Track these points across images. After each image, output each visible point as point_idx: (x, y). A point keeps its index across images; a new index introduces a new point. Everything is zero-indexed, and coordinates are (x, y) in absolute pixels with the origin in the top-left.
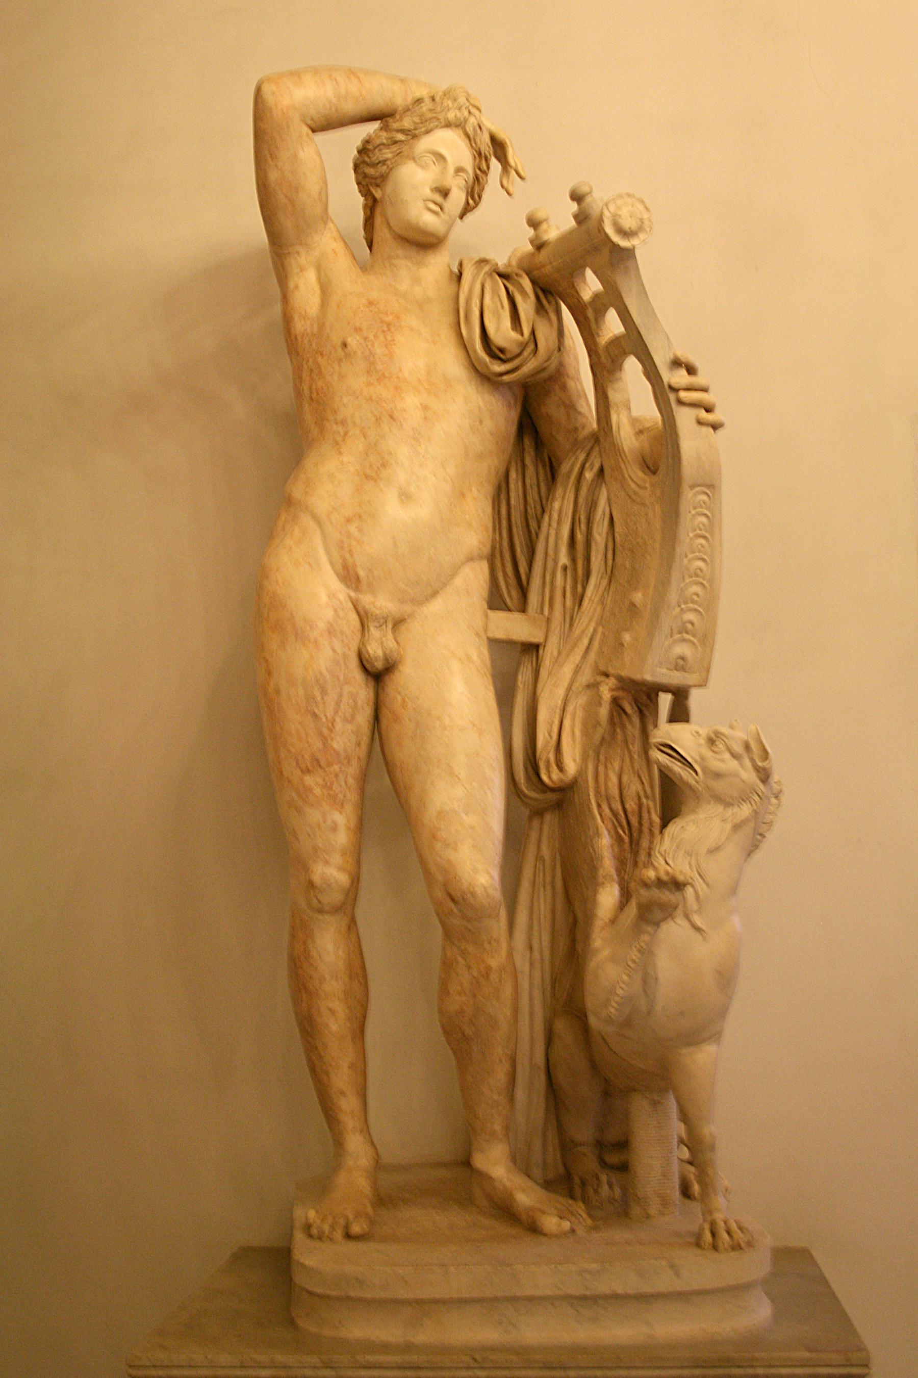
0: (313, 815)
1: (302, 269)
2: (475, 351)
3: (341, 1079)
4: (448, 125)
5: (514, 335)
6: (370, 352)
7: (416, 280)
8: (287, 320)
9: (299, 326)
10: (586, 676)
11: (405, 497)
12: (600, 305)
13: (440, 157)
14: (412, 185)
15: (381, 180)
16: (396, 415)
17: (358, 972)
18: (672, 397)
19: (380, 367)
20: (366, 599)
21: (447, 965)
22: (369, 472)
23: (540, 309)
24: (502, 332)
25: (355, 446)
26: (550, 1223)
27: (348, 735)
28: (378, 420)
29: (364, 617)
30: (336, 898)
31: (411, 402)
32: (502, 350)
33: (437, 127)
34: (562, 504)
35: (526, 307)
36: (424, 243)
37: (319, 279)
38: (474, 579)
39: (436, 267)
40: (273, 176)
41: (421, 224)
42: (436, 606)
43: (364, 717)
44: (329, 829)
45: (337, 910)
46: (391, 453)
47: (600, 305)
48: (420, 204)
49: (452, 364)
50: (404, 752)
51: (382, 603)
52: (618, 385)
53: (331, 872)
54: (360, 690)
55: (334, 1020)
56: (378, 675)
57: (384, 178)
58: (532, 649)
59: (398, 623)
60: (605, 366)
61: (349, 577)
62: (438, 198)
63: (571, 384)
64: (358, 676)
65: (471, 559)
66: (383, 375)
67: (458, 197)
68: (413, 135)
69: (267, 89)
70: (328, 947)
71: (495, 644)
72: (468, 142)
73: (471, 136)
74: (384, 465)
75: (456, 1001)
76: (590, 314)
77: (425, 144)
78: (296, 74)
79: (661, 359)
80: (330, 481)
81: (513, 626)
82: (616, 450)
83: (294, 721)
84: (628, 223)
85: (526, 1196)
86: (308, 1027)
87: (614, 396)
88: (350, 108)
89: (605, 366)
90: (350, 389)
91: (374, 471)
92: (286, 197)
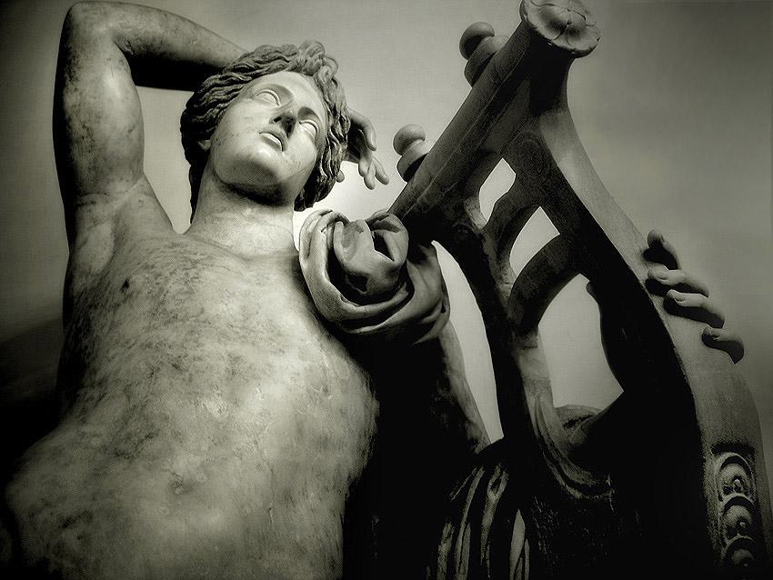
1: (96, 222)
2: (319, 282)
4: (296, 69)
5: (380, 256)
6: (161, 290)
12: (510, 220)
16: (185, 363)
18: (657, 302)
19: (171, 306)
22: (122, 446)
28: (153, 372)
32: (361, 279)
33: (283, 68)
37: (114, 231)
40: (71, 100)
41: (254, 155)
46: (166, 418)
47: (510, 220)
48: (255, 135)
52: (532, 354)
57: (214, 123)
60: (511, 326)
62: (278, 128)
63: (455, 381)
66: (175, 317)
72: (321, 93)
73: (325, 88)
74: (149, 436)
76: (489, 247)
79: (629, 248)
87: (528, 370)
89: (511, 326)
92: (84, 127)
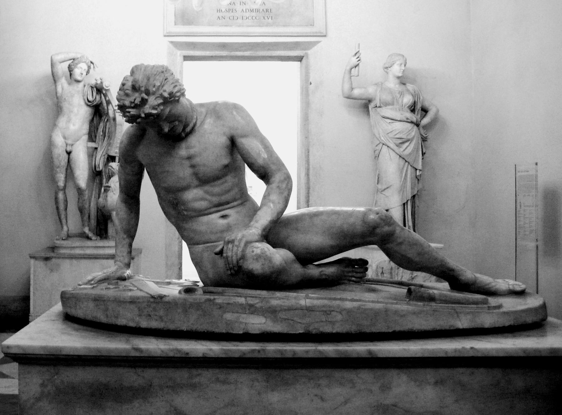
0: (58, 175)
3: (63, 217)
7: (78, 87)
8: (56, 93)
9: (58, 95)
10: (104, 154)
11: (74, 125)
13: (81, 68)
14: (78, 72)
15: (72, 71)
17: (66, 201)
20: (67, 141)
21: (79, 199)
23: (97, 93)
24: (91, 99)
25: (66, 116)
26: (94, 238)
27: (64, 162)
29: (67, 145)
30: (62, 188)
31: (75, 110)
34: (102, 125)
35: (95, 94)
36: (78, 81)
38: (86, 137)
39: (81, 85)
42: (78, 143)
43: (66, 160)
44: (61, 177)
45: (62, 190)
49: (82, 103)
50: (73, 166)
51: (69, 142)
53: (61, 184)
54: (66, 156)
55: (62, 207)
56: (69, 153)
58: (96, 148)
59: (72, 145)
61: (65, 138)
64: (65, 154)
65: (84, 135)
67: (85, 73)
68: (77, 64)
69: (53, 57)
70: (61, 196)
71: (88, 148)
75: (80, 205)
77: (79, 65)
78: (58, 54)
80: (62, 122)
81: (93, 145)
82: (109, 117)
83: (55, 160)
84: (107, 85)
85: (90, 235)
86: (58, 208)
88: (67, 59)
90: (65, 106)
91: (69, 121)
